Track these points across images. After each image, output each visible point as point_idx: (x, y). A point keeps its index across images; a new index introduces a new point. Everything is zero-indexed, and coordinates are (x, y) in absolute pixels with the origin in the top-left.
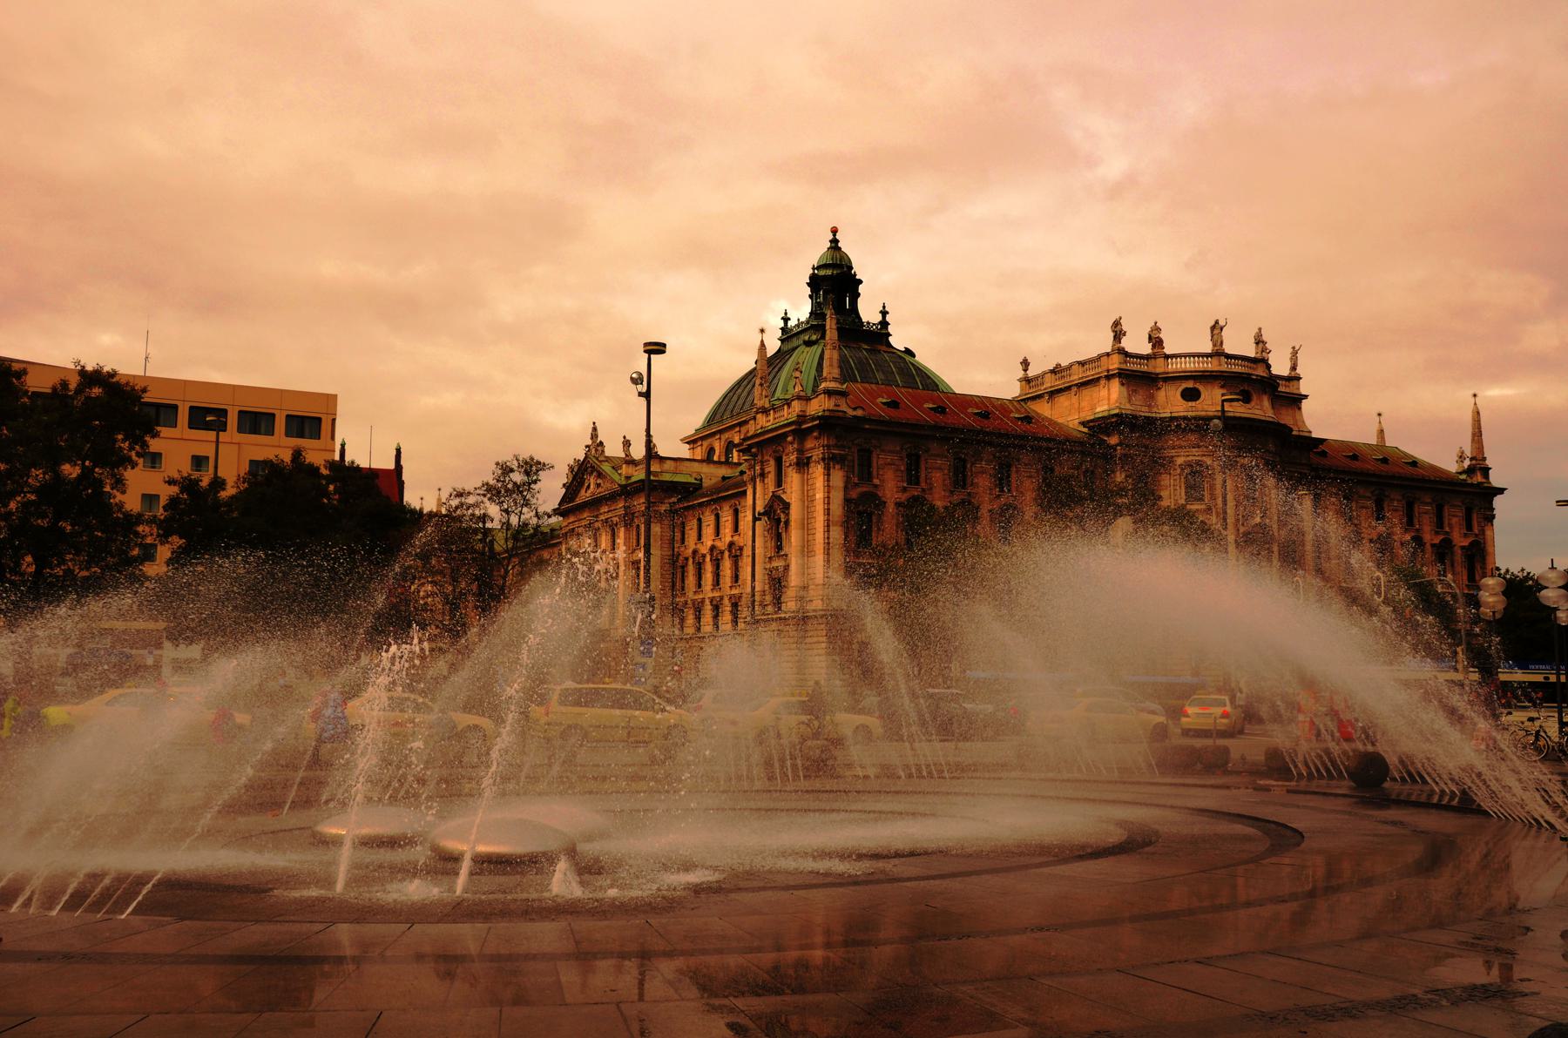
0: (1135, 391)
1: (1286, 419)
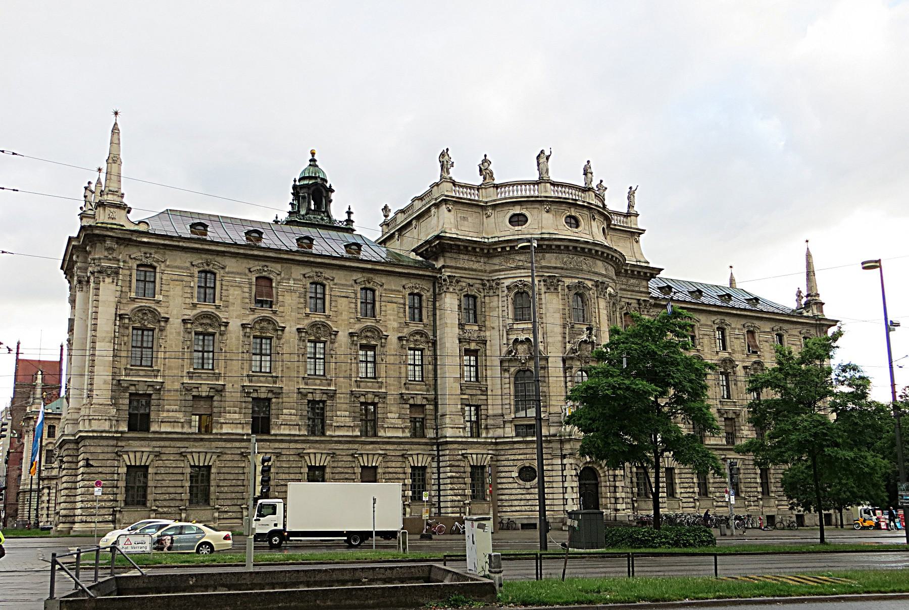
0: (464, 219)
1: (622, 246)
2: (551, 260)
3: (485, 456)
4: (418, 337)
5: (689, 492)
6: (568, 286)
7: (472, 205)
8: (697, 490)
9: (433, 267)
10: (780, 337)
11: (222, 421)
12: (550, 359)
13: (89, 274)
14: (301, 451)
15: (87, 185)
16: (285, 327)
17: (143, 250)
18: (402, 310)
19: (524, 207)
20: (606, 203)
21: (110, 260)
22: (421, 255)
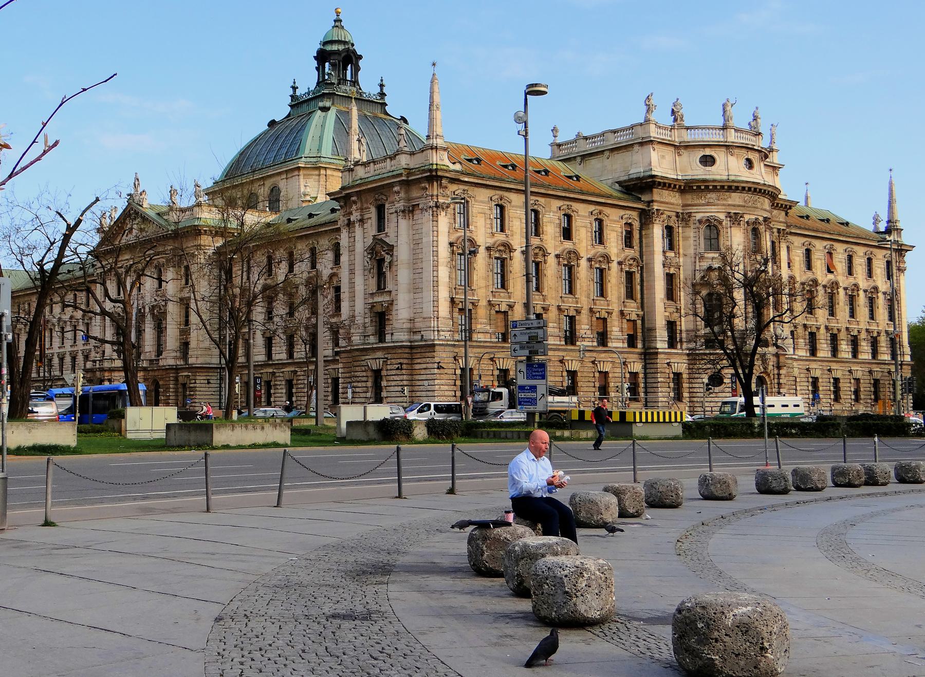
0: (663, 157)
18: (620, 238)
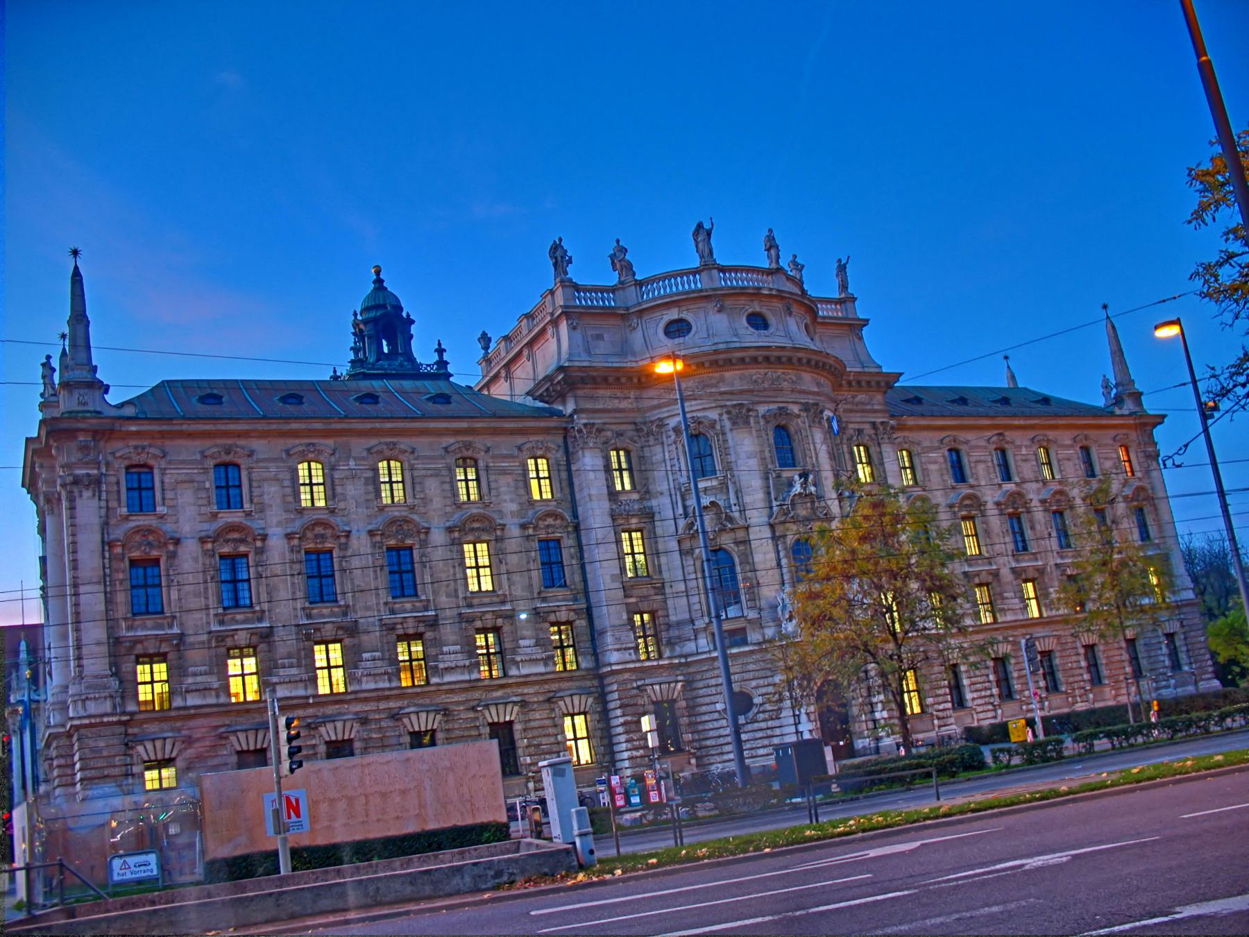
1: (839, 349)
2: (734, 379)
3: (672, 685)
4: (550, 521)
5: (985, 697)
6: (764, 416)
7: (607, 313)
8: (995, 691)
9: (560, 414)
10: (1086, 450)
11: (275, 679)
12: (751, 530)
13: (58, 488)
14: (396, 711)
15: (44, 361)
16: (350, 532)
17: (133, 443)
19: (684, 308)
20: (806, 287)
21: (87, 463)
22: (541, 398)
